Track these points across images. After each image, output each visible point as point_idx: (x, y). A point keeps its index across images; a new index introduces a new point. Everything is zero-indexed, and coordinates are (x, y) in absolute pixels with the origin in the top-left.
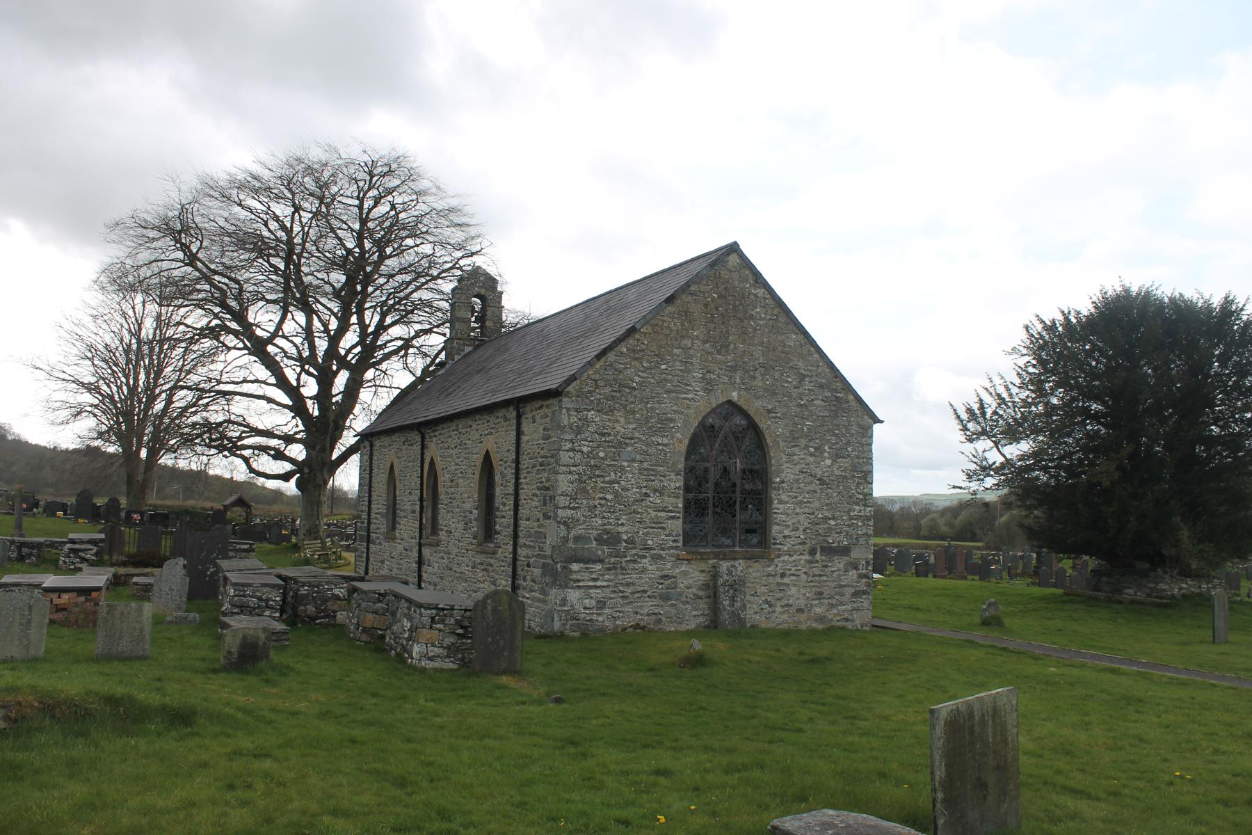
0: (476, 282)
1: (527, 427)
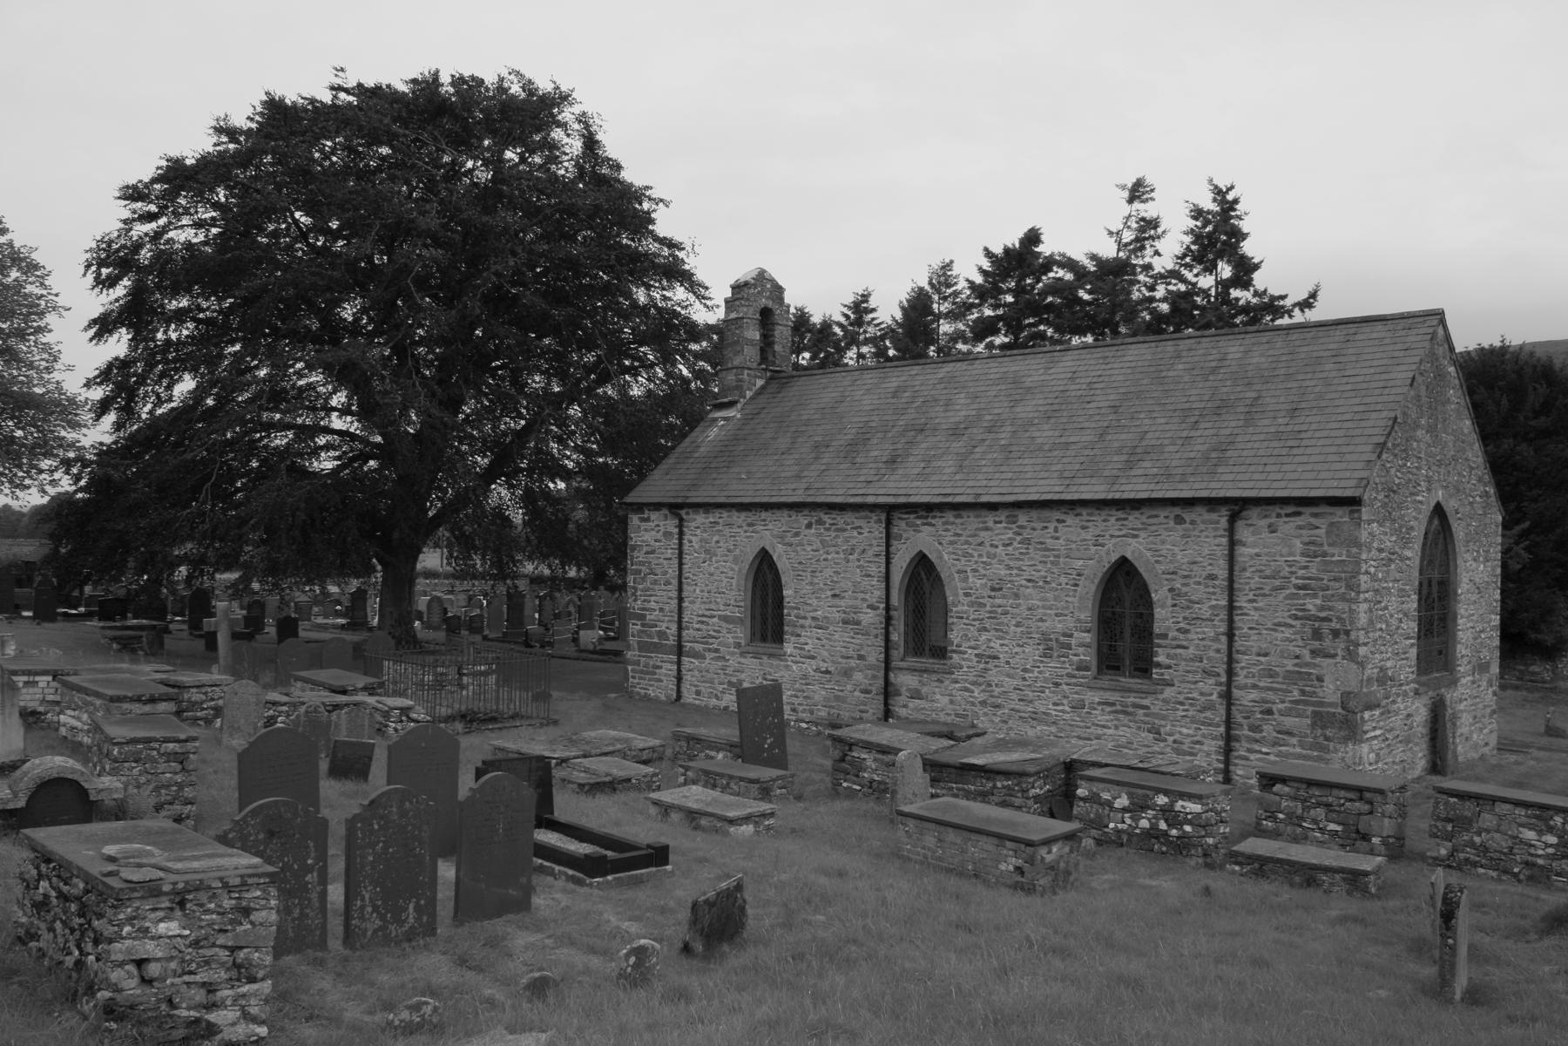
0: (763, 291)
1: (1243, 533)
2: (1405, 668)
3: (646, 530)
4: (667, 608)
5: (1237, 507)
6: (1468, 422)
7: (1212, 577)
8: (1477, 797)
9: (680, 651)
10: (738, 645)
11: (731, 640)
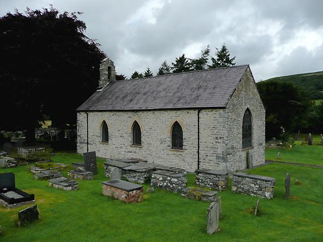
2: (240, 145)
5: (200, 109)
6: (256, 90)
7: (195, 125)
8: (242, 176)
9: (88, 143)
10: (99, 142)
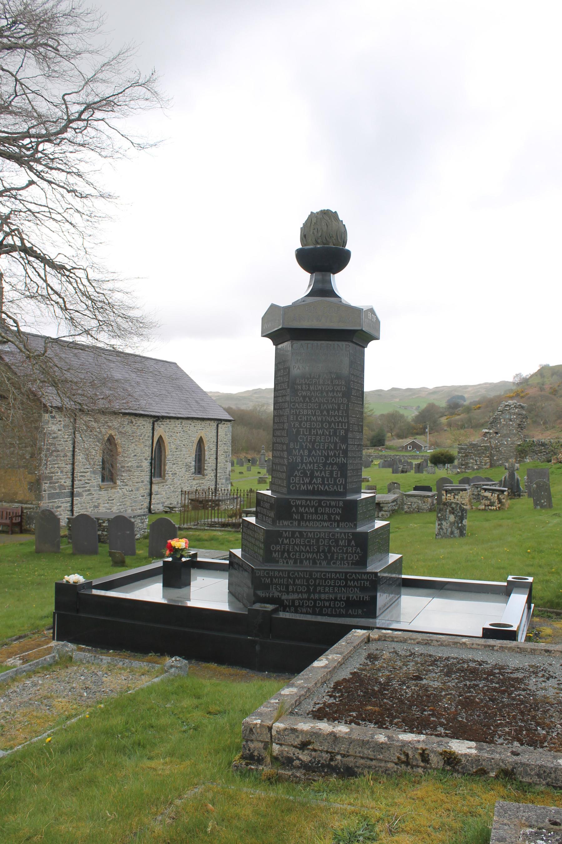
3: (53, 423)
4: (65, 470)
11: (95, 484)
